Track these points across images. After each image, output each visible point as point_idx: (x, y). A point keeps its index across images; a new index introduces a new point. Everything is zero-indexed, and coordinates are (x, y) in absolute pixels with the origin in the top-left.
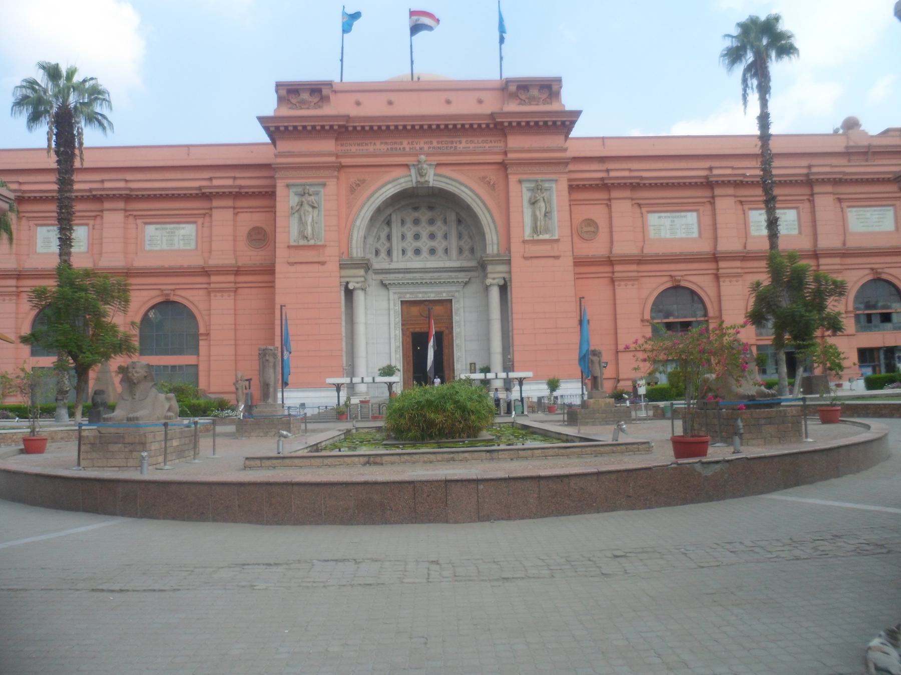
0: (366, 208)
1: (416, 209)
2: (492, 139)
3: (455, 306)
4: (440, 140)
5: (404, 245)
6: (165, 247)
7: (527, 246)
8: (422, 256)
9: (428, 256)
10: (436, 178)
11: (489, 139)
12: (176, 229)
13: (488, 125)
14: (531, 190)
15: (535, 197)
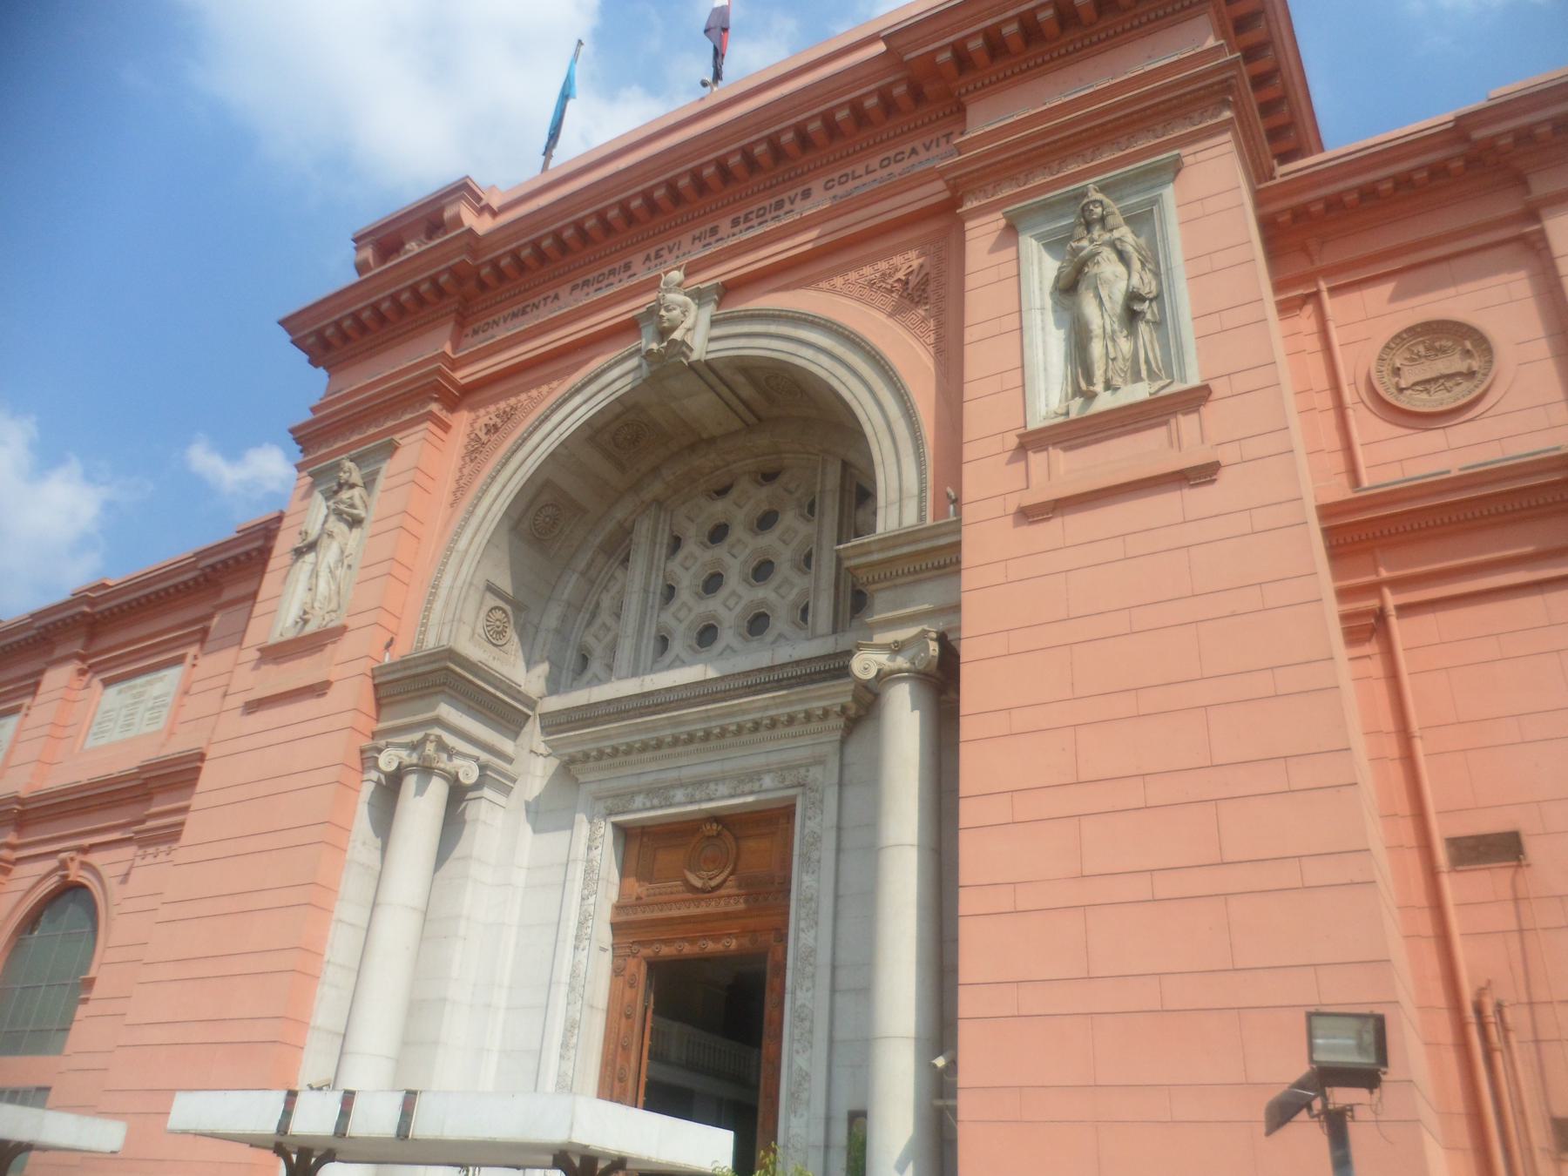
0: (494, 489)
1: (722, 492)
2: (918, 144)
3: (803, 827)
4: (742, 214)
5: (667, 618)
6: (117, 736)
7: (1036, 459)
8: (719, 645)
9: (736, 643)
10: (717, 332)
11: (907, 148)
12: (150, 683)
13: (884, 95)
14: (1054, 244)
15: (1076, 252)
